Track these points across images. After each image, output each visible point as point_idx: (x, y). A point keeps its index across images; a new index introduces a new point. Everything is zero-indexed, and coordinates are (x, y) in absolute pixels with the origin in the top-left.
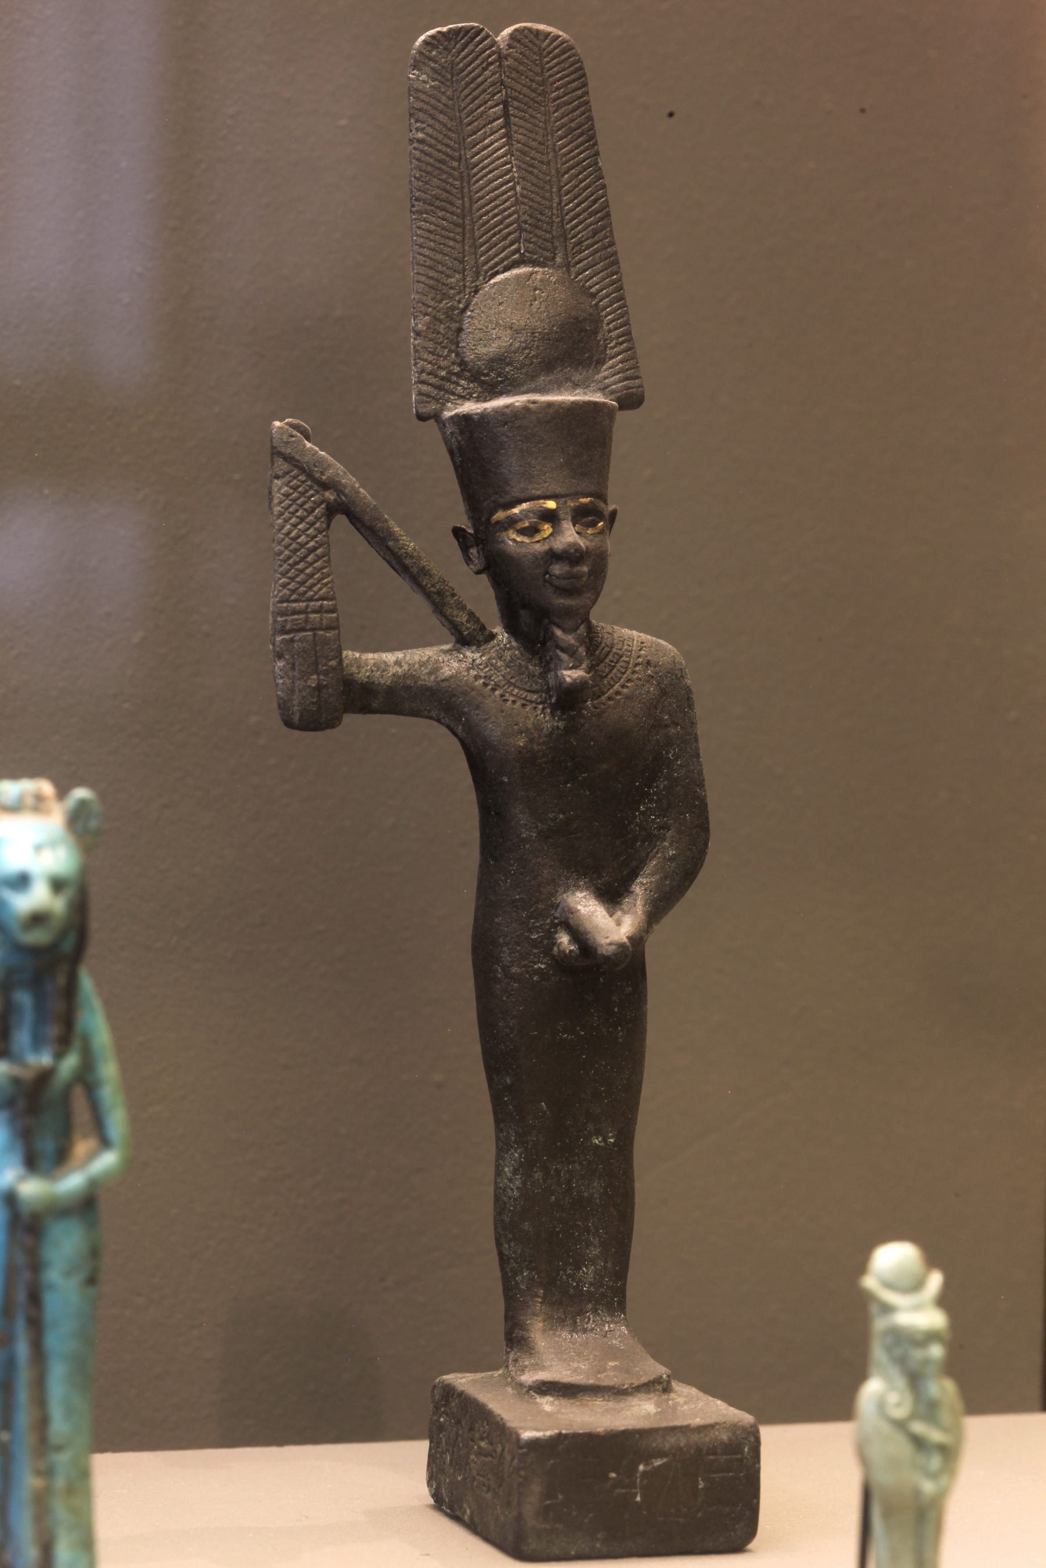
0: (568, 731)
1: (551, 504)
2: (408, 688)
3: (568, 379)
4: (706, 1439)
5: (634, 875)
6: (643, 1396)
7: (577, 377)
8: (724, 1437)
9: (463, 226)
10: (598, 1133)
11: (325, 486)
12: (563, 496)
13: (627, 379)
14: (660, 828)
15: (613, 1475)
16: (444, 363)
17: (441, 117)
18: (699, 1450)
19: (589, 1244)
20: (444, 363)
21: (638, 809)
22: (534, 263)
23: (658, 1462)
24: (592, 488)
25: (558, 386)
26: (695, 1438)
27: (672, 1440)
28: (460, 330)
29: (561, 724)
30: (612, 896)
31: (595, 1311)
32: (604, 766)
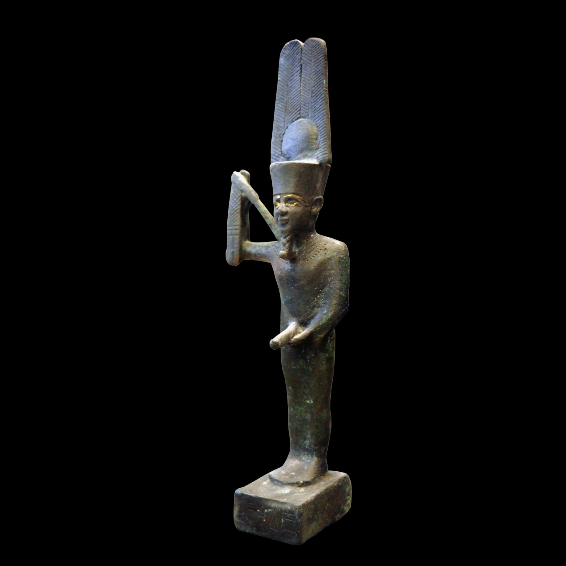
0: (291, 270)
1: (278, 197)
2: (259, 254)
3: (306, 155)
4: (284, 507)
5: (312, 318)
6: (289, 486)
7: (310, 154)
8: (289, 508)
9: (286, 107)
10: (308, 399)
11: (242, 191)
12: (283, 194)
13: (323, 154)
14: (324, 304)
15: (258, 511)
16: (277, 152)
17: (285, 72)
18: (281, 510)
19: (308, 434)
20: (277, 152)
21: (316, 297)
22: (304, 117)
23: (270, 510)
24: (292, 191)
25: (305, 156)
26: (280, 506)
27: (274, 505)
28: (282, 141)
29: (290, 268)
30: (303, 324)
31: (308, 455)
32: (302, 282)
